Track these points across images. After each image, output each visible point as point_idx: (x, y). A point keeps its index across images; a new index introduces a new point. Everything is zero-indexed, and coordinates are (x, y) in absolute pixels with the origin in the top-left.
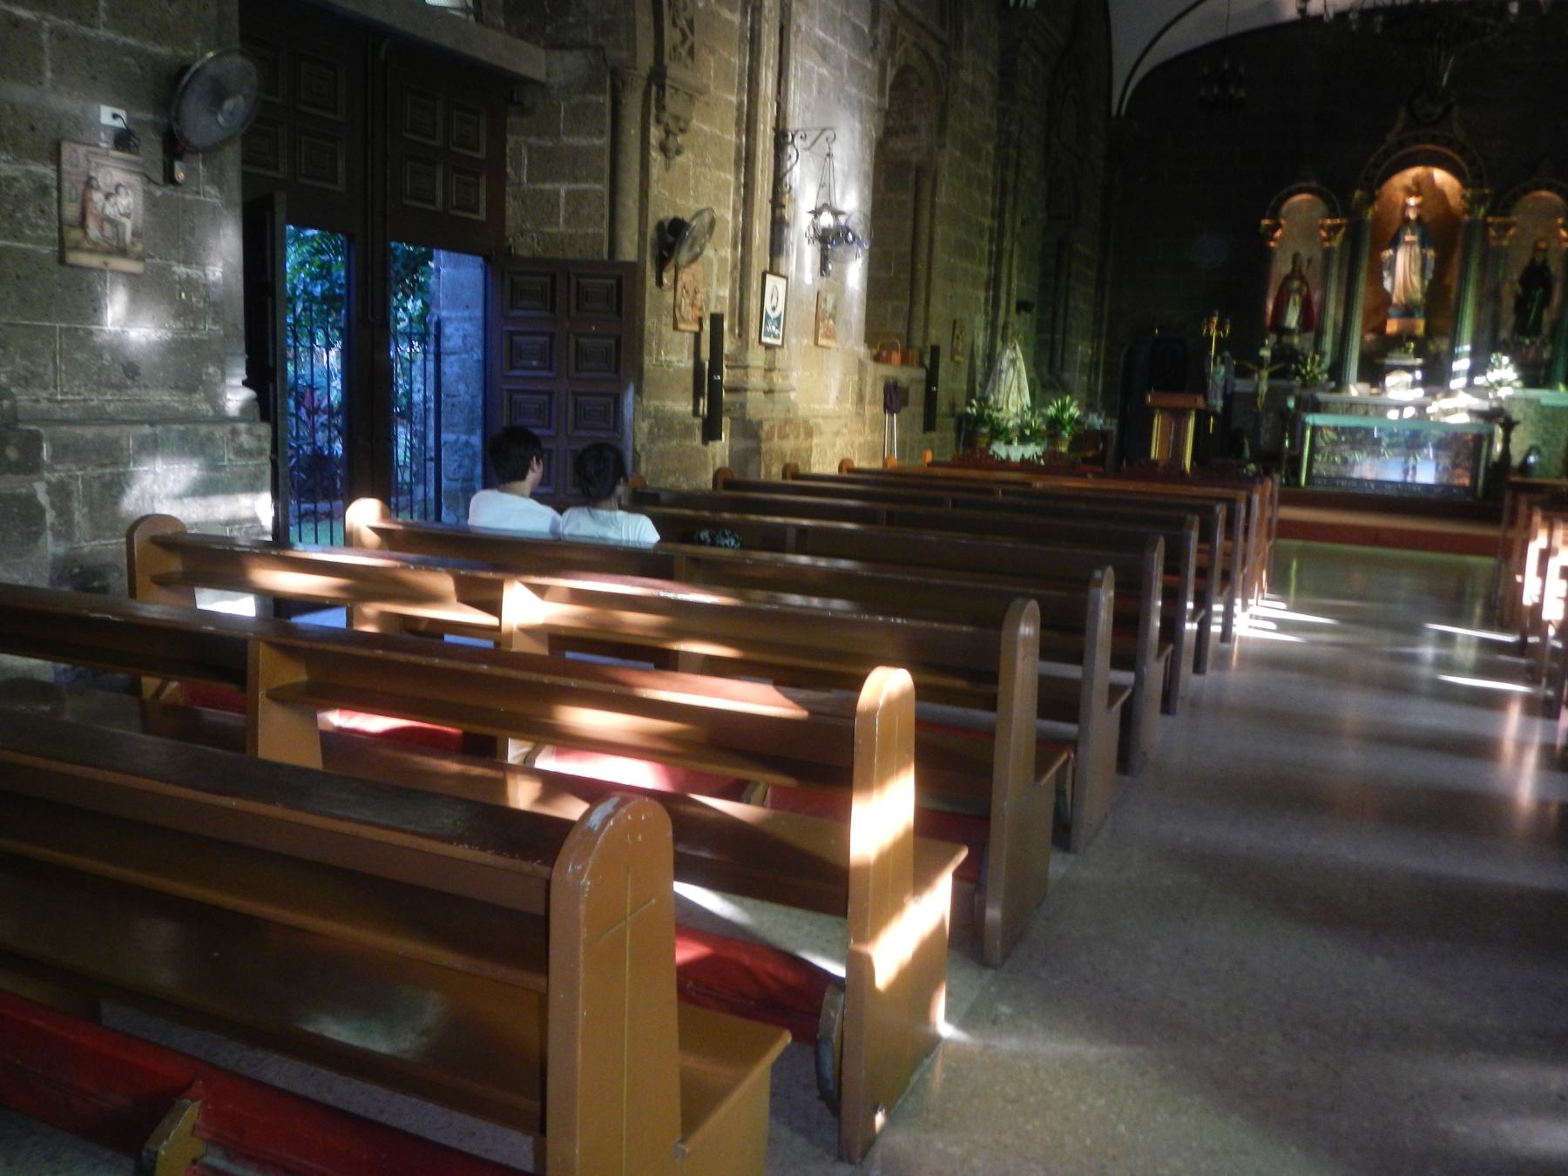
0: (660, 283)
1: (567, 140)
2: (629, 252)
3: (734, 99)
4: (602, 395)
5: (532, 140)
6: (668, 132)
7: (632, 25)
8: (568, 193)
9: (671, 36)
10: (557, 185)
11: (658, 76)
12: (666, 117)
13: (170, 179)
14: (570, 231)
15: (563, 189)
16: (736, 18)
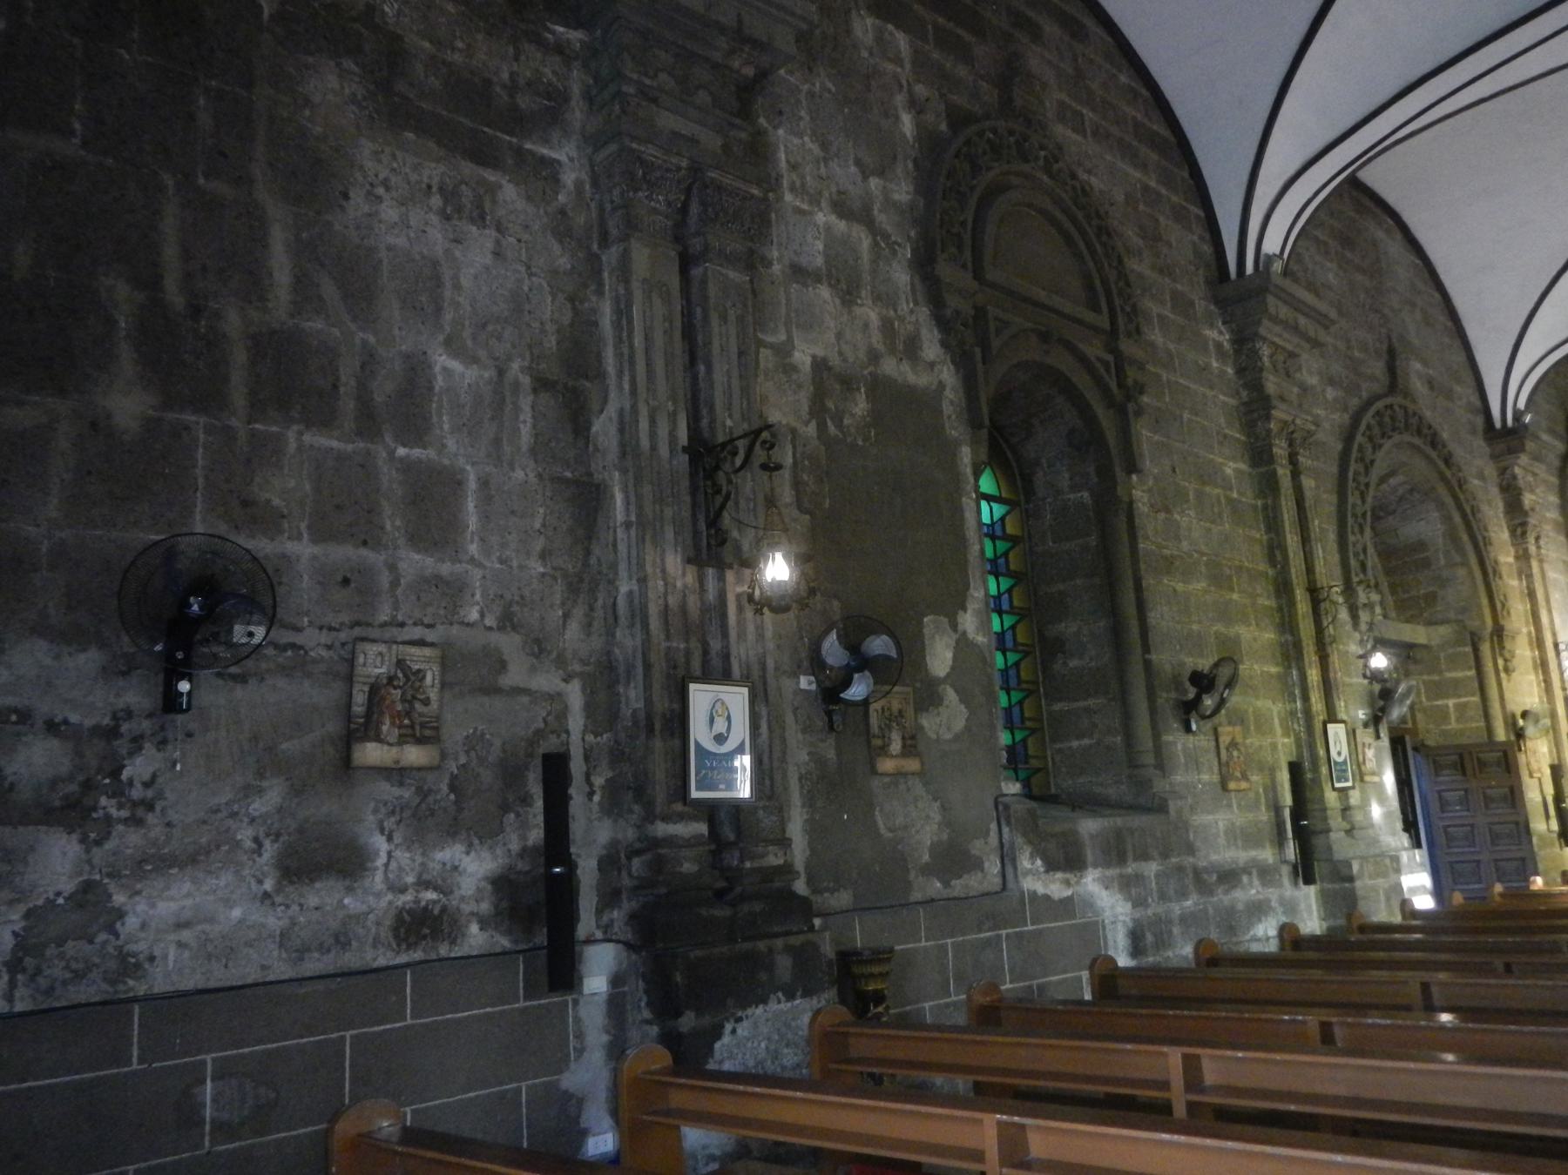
0: (1520, 750)
1: (1448, 675)
2: (1501, 734)
3: (1525, 630)
4: (1463, 825)
5: (1425, 677)
6: (1506, 660)
7: (1479, 606)
8: (1455, 705)
9: (1499, 606)
10: (1446, 701)
11: (1499, 633)
12: (1507, 655)
13: (1378, 737)
14: (1461, 726)
15: (1451, 703)
16: (1514, 583)
